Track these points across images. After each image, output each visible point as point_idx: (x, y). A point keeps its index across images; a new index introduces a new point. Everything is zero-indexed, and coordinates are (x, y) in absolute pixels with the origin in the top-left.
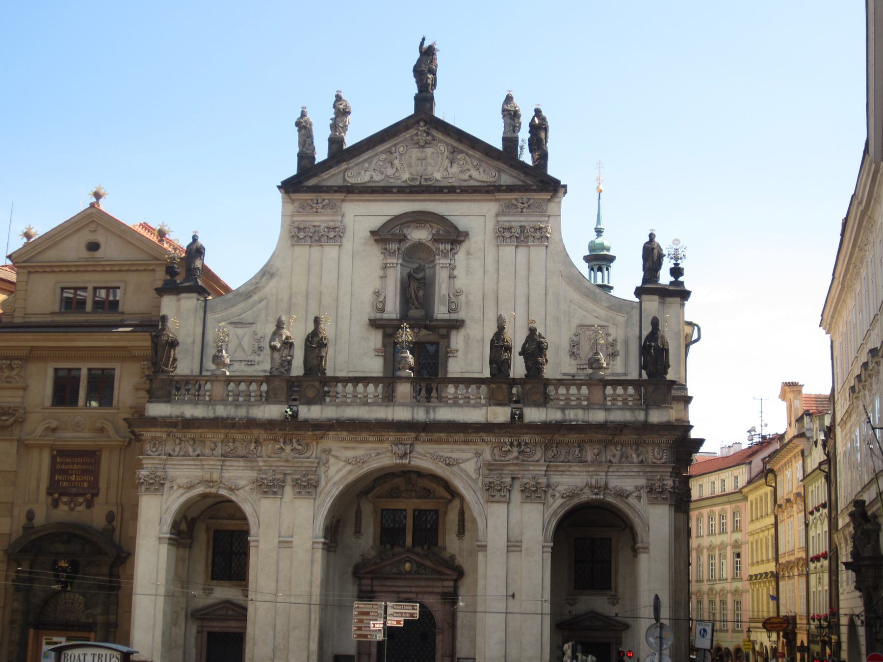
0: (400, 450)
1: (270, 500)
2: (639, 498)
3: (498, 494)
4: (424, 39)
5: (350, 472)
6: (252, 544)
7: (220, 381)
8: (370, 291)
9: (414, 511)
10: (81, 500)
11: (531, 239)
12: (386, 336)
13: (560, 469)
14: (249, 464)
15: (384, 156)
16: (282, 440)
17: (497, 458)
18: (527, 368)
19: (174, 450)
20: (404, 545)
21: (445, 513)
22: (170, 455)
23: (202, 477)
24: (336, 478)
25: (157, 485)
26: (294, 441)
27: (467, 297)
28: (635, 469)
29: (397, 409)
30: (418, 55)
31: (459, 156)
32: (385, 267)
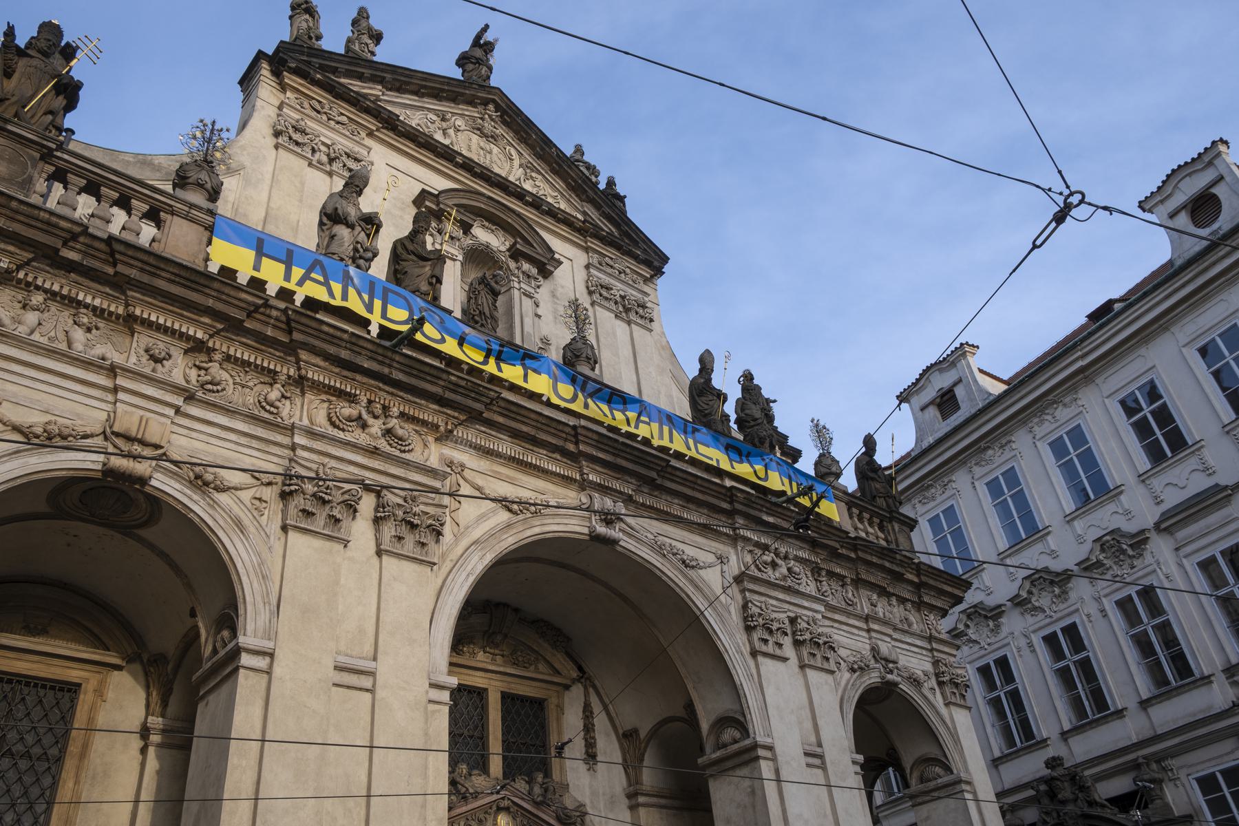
1: (317, 543)
4: (487, 26)
5: (509, 526)
6: (246, 659)
7: (192, 220)
9: (506, 697)
11: (632, 316)
13: (837, 617)
14: (260, 432)
15: (432, 116)
16: (364, 400)
20: (485, 769)
21: (560, 708)
23: (110, 421)
24: (477, 533)
26: (395, 411)
28: (918, 643)
30: (466, 46)
31: (534, 175)
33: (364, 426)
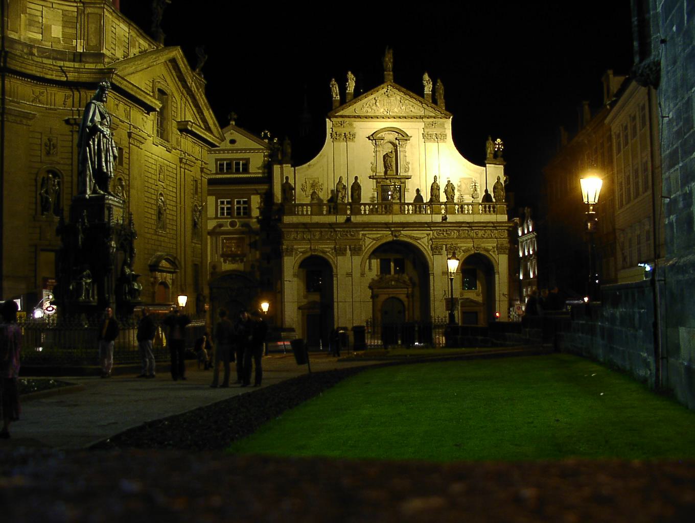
0: (397, 234)
2: (494, 251)
3: (437, 251)
6: (334, 276)
8: (370, 162)
10: (238, 258)
12: (377, 182)
17: (437, 236)
18: (447, 198)
19: (297, 236)
20: (390, 274)
22: (296, 239)
25: (290, 252)
27: (412, 164)
29: (394, 216)
32: (376, 152)
33: (347, 235)
